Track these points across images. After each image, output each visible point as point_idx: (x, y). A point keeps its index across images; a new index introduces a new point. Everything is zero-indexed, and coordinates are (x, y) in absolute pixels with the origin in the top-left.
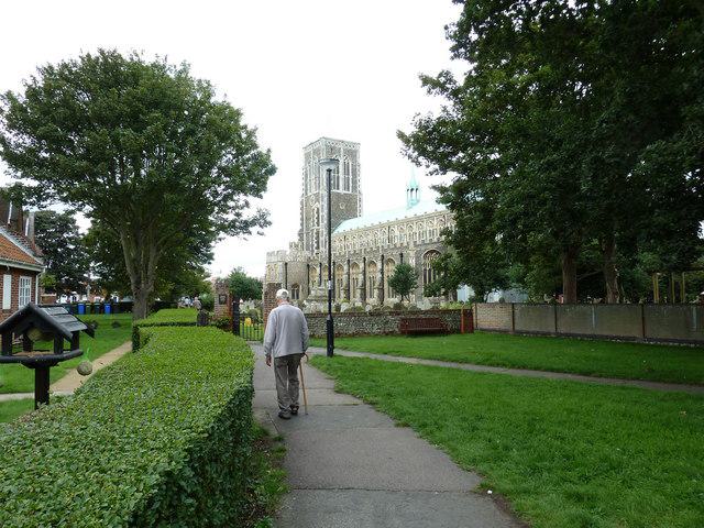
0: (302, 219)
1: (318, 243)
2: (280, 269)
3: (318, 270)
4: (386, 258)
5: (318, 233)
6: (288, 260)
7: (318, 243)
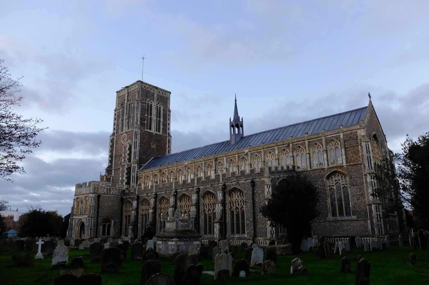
1: (128, 178)
2: (91, 202)
3: (135, 203)
4: (229, 189)
6: (100, 191)
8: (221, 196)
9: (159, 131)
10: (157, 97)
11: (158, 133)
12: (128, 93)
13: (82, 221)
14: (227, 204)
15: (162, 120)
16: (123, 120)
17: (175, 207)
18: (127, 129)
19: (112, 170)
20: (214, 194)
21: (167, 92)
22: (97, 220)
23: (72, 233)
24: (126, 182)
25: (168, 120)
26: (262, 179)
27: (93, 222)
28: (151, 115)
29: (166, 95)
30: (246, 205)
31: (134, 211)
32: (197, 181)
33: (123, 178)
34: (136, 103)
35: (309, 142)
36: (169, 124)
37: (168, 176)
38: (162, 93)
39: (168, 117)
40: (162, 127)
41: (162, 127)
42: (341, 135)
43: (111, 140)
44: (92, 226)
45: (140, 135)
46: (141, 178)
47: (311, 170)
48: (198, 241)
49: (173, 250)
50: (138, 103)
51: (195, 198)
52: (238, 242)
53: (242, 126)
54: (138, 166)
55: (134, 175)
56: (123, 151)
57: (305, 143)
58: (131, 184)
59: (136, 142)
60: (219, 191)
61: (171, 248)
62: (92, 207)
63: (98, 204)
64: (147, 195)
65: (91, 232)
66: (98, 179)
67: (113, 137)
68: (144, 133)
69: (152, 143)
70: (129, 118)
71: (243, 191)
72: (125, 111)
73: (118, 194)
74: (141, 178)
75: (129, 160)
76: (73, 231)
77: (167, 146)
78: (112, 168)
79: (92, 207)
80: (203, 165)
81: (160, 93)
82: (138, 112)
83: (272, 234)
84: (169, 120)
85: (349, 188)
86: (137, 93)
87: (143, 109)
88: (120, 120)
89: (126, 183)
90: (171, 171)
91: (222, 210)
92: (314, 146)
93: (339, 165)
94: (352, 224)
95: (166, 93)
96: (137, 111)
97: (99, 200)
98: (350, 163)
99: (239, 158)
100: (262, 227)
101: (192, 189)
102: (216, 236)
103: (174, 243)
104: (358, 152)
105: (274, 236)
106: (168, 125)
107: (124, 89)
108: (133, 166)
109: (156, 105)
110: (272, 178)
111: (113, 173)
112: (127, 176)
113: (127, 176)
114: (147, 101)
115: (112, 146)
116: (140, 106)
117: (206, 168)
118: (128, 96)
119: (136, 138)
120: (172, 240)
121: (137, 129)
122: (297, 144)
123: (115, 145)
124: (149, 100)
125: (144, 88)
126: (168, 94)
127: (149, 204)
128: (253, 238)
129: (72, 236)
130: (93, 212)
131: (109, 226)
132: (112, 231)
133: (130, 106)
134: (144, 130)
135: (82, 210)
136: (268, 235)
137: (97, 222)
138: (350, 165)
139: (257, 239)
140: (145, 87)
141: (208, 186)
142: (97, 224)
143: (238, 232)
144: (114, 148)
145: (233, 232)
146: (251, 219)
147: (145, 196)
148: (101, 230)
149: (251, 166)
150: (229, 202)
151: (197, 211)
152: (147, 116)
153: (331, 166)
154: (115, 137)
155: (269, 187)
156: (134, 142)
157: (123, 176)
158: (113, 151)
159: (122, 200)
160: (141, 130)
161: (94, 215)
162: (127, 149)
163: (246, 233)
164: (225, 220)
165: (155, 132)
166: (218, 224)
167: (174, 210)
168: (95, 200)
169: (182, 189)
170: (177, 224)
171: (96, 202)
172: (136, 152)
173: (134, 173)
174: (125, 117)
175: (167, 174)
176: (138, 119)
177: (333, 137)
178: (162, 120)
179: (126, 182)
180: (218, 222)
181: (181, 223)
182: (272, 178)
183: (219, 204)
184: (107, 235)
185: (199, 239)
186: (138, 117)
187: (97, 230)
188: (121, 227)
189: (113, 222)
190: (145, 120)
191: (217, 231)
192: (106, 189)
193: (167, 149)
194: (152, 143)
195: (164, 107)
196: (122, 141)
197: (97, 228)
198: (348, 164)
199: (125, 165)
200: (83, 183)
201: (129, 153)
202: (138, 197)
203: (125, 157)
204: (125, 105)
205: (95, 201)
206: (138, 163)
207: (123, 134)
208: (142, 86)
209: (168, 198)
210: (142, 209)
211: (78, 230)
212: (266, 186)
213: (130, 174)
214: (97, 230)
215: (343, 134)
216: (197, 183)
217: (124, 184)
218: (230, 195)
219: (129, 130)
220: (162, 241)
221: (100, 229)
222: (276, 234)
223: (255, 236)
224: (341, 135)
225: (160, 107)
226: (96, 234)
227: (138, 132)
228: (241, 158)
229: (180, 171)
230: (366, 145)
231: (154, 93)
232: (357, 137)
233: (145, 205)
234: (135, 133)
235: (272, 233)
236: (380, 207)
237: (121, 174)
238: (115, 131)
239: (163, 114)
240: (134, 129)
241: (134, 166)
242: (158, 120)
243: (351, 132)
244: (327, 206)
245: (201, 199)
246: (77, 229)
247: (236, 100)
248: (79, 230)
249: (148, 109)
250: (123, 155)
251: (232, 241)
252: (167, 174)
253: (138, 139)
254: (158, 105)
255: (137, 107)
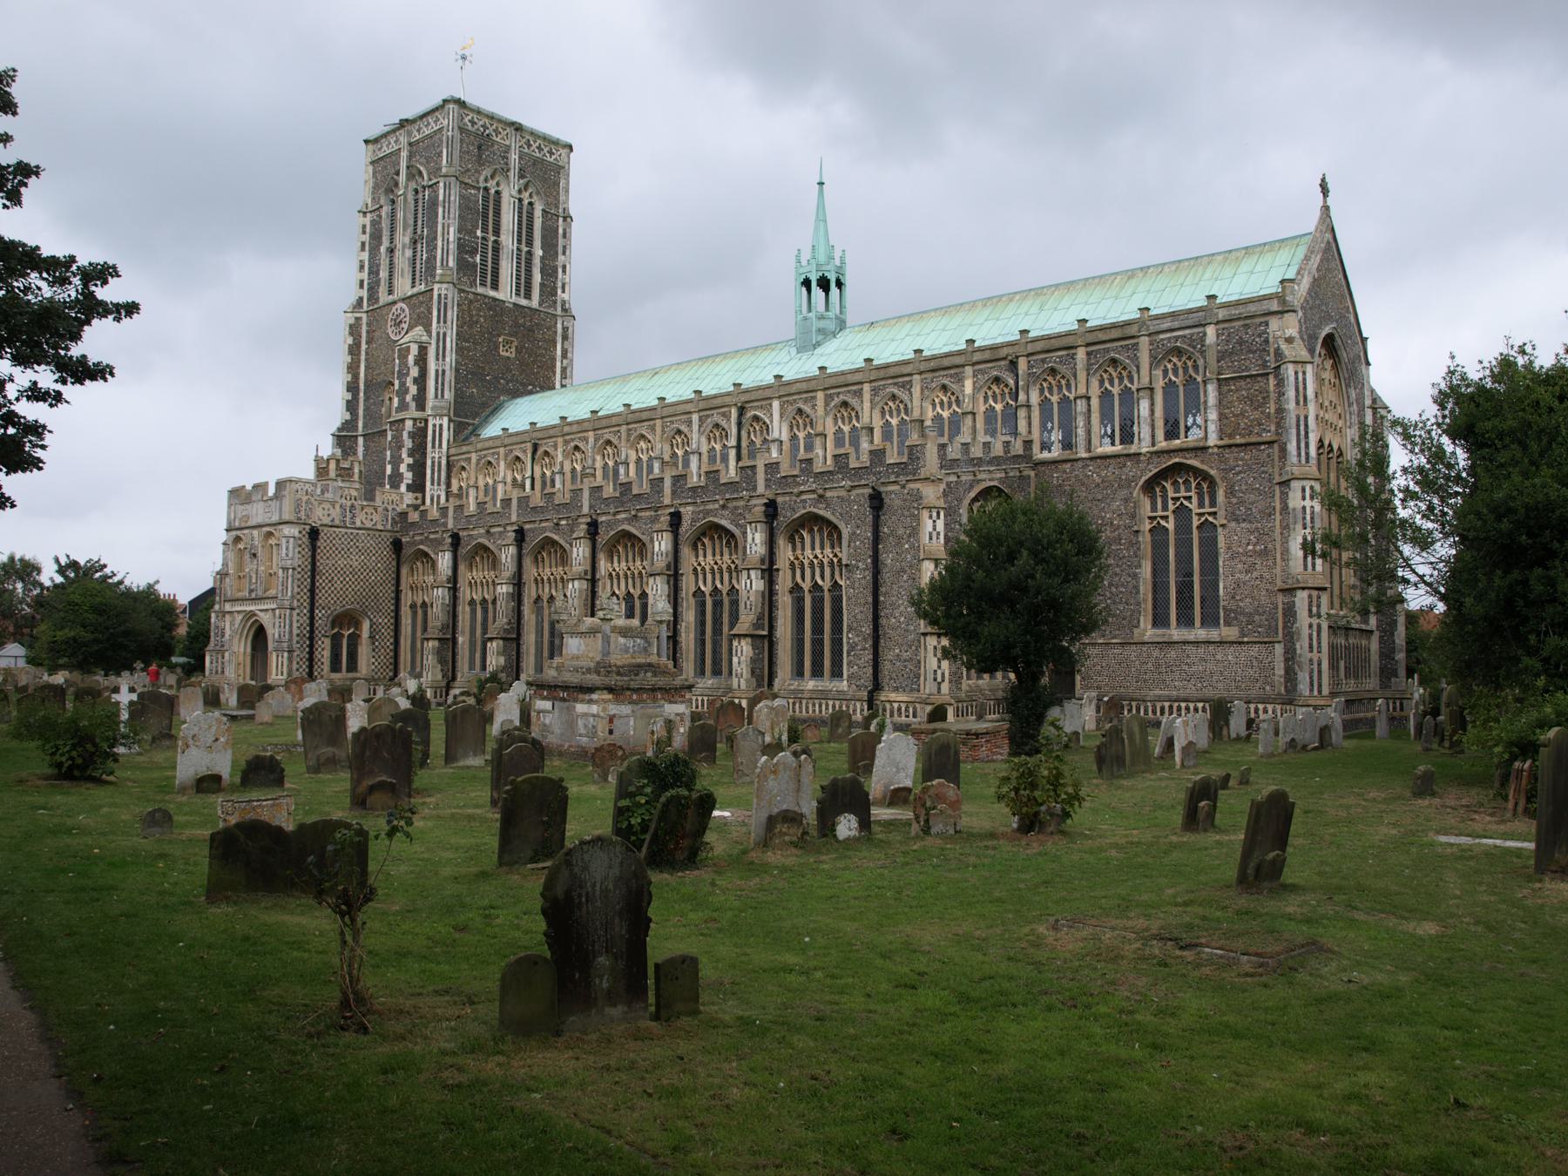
0: (352, 387)
1: (419, 469)
3: (444, 561)
4: (786, 516)
5: (420, 435)
6: (320, 516)
7: (419, 469)
8: (758, 540)
9: (528, 296)
10: (519, 163)
11: (524, 302)
12: (410, 144)
13: (256, 621)
14: (781, 572)
15: (538, 252)
16: (391, 251)
17: (589, 577)
18: (409, 282)
19: (357, 436)
20: (733, 536)
21: (556, 143)
22: (312, 618)
23: (223, 663)
24: (410, 482)
25: (560, 250)
26: (912, 485)
27: (295, 625)
28: (497, 232)
29: (553, 157)
30: (848, 578)
31: (440, 589)
32: (674, 485)
33: (398, 470)
34: (441, 185)
35: (1088, 354)
36: (564, 267)
37: (562, 464)
38: (539, 148)
39: (561, 241)
40: (537, 278)
41: (537, 278)
42: (1211, 331)
43: (351, 326)
44: (295, 639)
45: (455, 308)
46: (463, 468)
47: (1091, 459)
48: (682, 702)
49: (593, 733)
50: (447, 187)
51: (663, 548)
52: (817, 706)
53: (839, 284)
54: (452, 425)
55: (437, 456)
56: (397, 369)
57: (1073, 357)
58: (428, 489)
59: (445, 334)
60: (753, 525)
61: (586, 726)
62: (291, 571)
63: (313, 564)
64: (488, 532)
65: (290, 661)
66: (309, 473)
67: (358, 315)
68: (471, 302)
69: (501, 340)
70: (415, 242)
71: (841, 525)
72: (400, 215)
73: (382, 528)
74: (463, 468)
75: (421, 402)
76: (227, 654)
77: (559, 352)
78: (357, 430)
79: (291, 571)
80: (695, 427)
81: (529, 146)
82: (451, 221)
83: (939, 684)
84: (564, 253)
85: (1220, 530)
86: (445, 144)
87: (466, 207)
88: (383, 249)
89: (409, 488)
90: (572, 444)
91: (763, 593)
92: (1106, 371)
93: (1191, 445)
94: (1219, 657)
95: (553, 147)
96: (444, 218)
97: (314, 548)
98: (1231, 436)
99: (827, 404)
100: (905, 655)
101: (653, 513)
102: (739, 681)
103: (594, 709)
104: (1264, 398)
105: (945, 687)
106: (560, 270)
107: (394, 131)
108: (434, 426)
109: (514, 193)
110: (948, 484)
111: (360, 450)
112: (410, 461)
113: (410, 461)
114: (482, 178)
115: (354, 350)
116: (455, 198)
117: (703, 439)
118: (410, 157)
119: (442, 319)
120: (587, 697)
121: (445, 286)
122: (1043, 361)
123: (364, 346)
124: (487, 172)
125: (470, 128)
126: (563, 152)
127: (495, 563)
128: (871, 693)
129: (223, 672)
130: (296, 590)
131: (354, 640)
132: (365, 657)
133: (420, 196)
134: (473, 290)
135: (254, 581)
136: (922, 686)
137: (312, 624)
138: (1230, 446)
139: (883, 699)
140: (473, 123)
141: (711, 506)
142: (312, 632)
143: (817, 672)
144: (363, 357)
145: (799, 672)
146: (867, 629)
147: (480, 536)
148: (327, 653)
149: (872, 437)
150: (787, 563)
151: (669, 596)
152: (483, 238)
153: (1162, 444)
154: (364, 316)
155: (935, 514)
156: (434, 334)
157: (396, 461)
158: (359, 366)
159: (397, 546)
160: (461, 291)
161: (298, 600)
162: (411, 359)
163: (845, 676)
164: (772, 628)
165: (514, 299)
166: (747, 643)
167: (585, 587)
168: (300, 546)
169: (614, 514)
170: (606, 640)
171: (303, 553)
172: (444, 371)
173: (437, 451)
174: (403, 238)
175: (560, 458)
176: (451, 246)
177: (1177, 338)
178: (540, 253)
179: (410, 482)
180: (745, 636)
181: (622, 640)
182: (948, 484)
183: (753, 573)
184: (348, 670)
185: (683, 696)
186: (451, 239)
187: (311, 653)
188: (397, 643)
189: (366, 625)
190: (473, 252)
191: (743, 666)
192: (337, 506)
193: (558, 364)
194: (501, 340)
195: (547, 204)
196: (390, 331)
197: (311, 646)
198: (1226, 441)
199: (403, 421)
200: (256, 487)
201: (416, 375)
202: (456, 538)
203: (403, 391)
204: (401, 192)
205: (300, 549)
206: (452, 415)
207: (394, 303)
208: (463, 118)
209: (567, 546)
210: (470, 582)
211: (245, 653)
212: (925, 513)
213: (424, 454)
214: (311, 653)
215: (1217, 330)
216: (674, 493)
217: (403, 488)
218: (792, 539)
219: (415, 290)
220: (554, 699)
221: (323, 649)
222: (950, 682)
223: (877, 686)
224: (1211, 331)
225: (531, 204)
226: (311, 667)
227: (450, 296)
228: (835, 406)
229: (608, 448)
230: (1296, 373)
231: (509, 146)
232: (1267, 341)
233: (480, 567)
234: (439, 303)
235: (939, 679)
236: (1325, 598)
237: (388, 453)
238: (365, 293)
239: (544, 229)
240: (436, 287)
241: (438, 422)
242: (523, 253)
243: (1248, 322)
244: (1136, 588)
245: (686, 551)
246: (242, 650)
247: (821, 184)
248: (249, 650)
249: (486, 207)
250: (397, 383)
251: (794, 704)
252: (560, 458)
253: (449, 323)
254: (525, 195)
255: (444, 201)
